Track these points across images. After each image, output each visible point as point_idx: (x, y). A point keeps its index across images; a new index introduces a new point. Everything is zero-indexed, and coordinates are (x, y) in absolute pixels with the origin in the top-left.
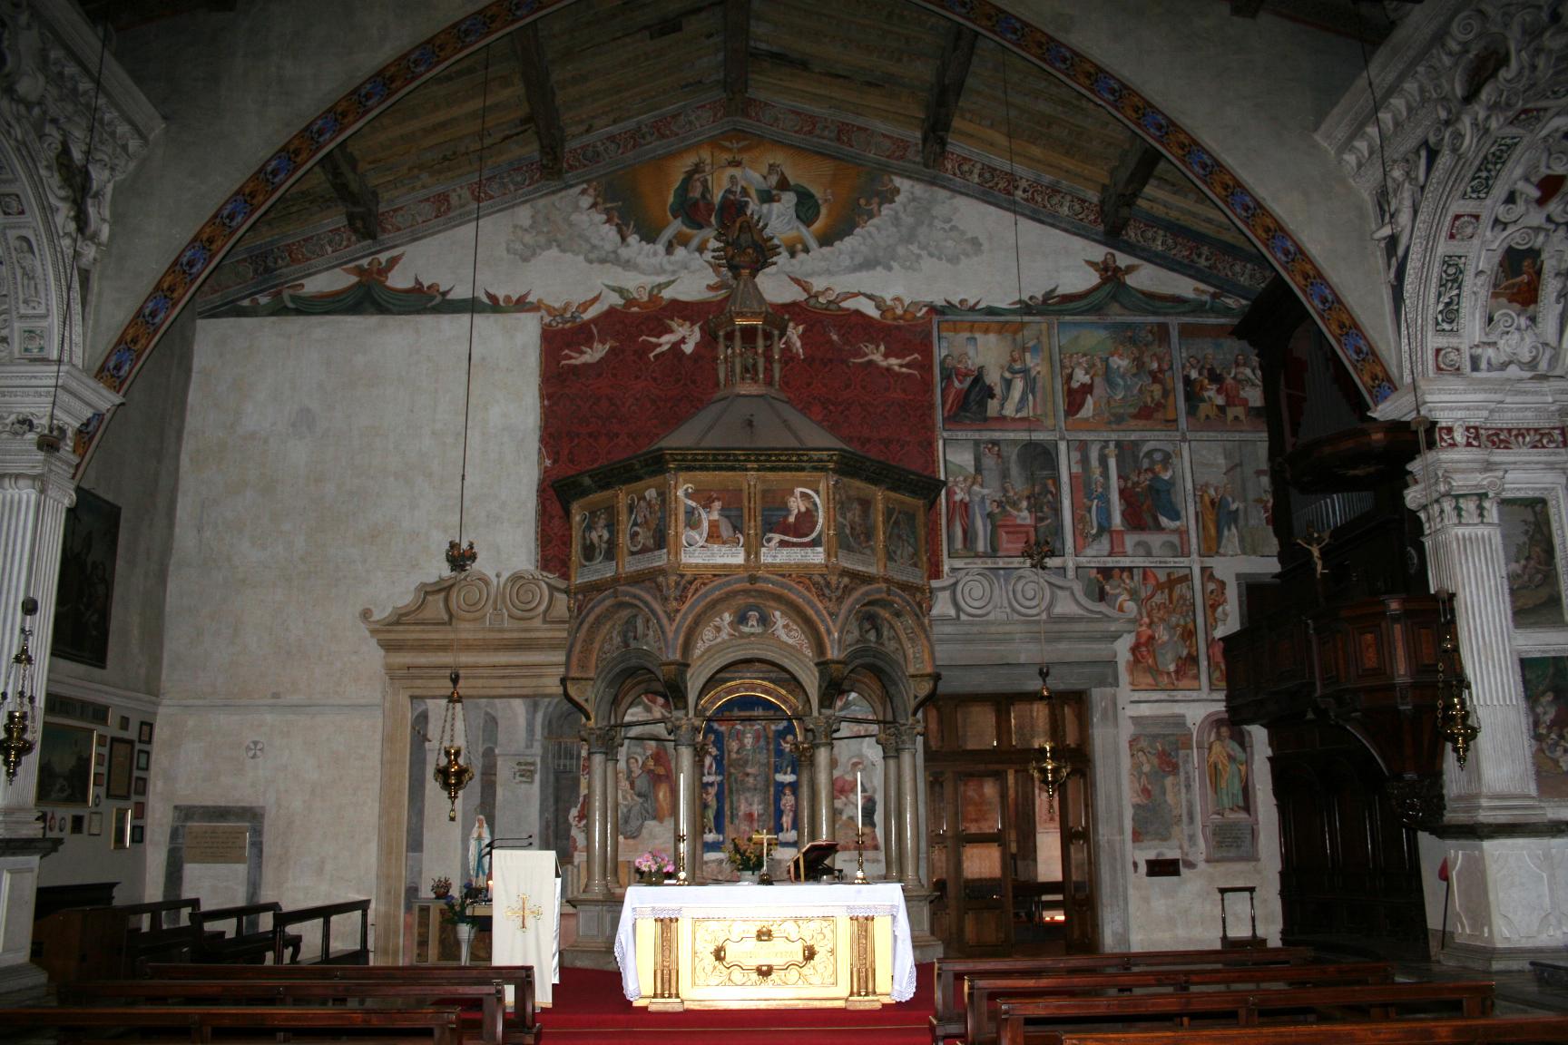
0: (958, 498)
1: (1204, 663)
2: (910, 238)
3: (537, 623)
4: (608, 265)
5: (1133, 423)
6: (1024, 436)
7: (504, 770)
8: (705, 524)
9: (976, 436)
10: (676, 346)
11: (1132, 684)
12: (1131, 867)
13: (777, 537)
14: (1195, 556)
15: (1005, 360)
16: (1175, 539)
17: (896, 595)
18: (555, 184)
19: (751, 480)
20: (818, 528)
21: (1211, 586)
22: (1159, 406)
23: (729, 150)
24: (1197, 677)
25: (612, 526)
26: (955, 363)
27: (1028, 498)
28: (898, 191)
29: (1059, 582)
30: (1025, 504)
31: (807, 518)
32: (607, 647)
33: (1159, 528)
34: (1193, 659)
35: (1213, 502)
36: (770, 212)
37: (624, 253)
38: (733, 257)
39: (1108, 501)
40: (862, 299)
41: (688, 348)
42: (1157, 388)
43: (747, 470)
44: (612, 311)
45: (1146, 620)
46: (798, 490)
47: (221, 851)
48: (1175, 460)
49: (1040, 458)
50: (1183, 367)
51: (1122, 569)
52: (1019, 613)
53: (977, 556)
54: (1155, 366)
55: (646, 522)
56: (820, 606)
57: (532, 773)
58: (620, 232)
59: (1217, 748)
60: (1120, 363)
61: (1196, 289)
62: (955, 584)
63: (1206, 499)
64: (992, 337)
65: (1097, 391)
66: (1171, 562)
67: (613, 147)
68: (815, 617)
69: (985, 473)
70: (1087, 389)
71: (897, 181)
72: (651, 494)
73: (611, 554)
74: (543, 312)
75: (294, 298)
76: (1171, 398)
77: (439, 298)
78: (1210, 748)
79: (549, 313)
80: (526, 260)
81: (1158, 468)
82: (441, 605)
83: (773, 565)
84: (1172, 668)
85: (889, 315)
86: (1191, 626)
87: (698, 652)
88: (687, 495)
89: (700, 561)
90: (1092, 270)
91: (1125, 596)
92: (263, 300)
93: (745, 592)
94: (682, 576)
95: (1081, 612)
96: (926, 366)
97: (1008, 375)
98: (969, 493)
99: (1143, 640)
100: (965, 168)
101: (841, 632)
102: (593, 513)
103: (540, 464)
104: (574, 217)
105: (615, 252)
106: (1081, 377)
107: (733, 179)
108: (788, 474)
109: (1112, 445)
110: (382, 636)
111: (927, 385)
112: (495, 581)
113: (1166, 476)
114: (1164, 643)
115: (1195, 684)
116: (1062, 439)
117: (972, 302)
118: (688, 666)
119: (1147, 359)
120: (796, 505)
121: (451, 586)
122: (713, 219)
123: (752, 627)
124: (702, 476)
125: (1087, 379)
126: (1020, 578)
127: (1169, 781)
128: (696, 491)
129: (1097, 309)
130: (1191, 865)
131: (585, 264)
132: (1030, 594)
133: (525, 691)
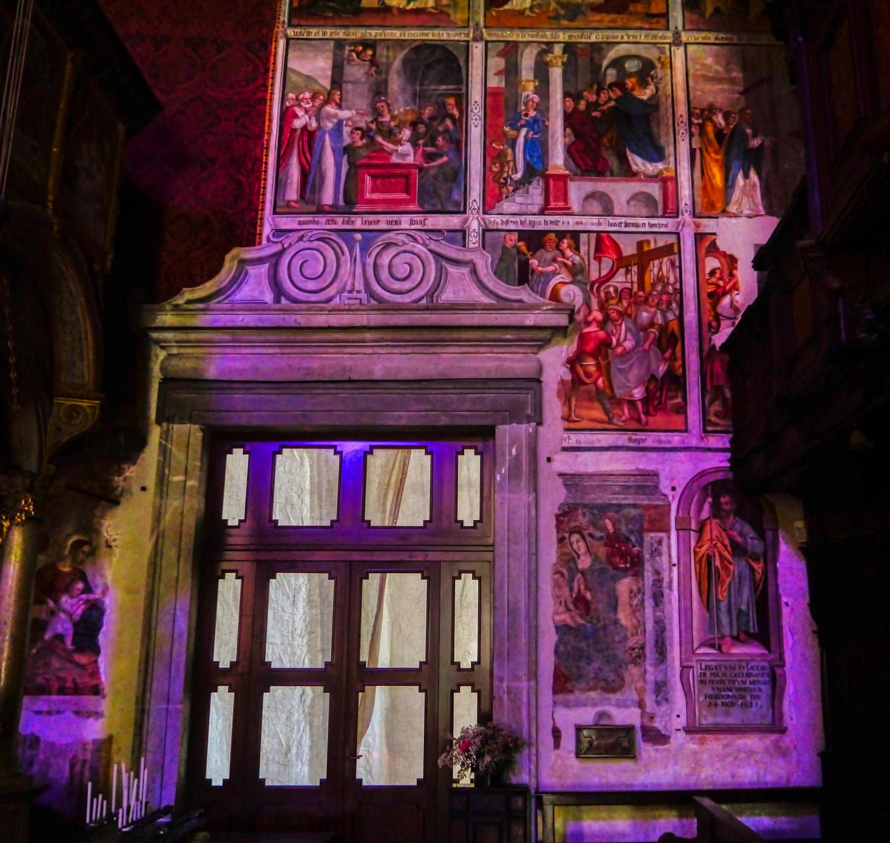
0: (298, 124)
1: (694, 394)
6: (415, 34)
9: (341, 34)
11: (567, 418)
12: (549, 740)
14: (687, 217)
16: (654, 189)
21: (712, 263)
24: (682, 409)
27: (414, 125)
30: (407, 133)
33: (630, 174)
34: (675, 381)
35: (719, 134)
45: (598, 315)
48: (659, 72)
49: (440, 66)
52: (380, 300)
53: (321, 210)
59: (713, 530)
62: (279, 255)
66: (645, 223)
69: (348, 87)
78: (700, 531)
81: (630, 82)
84: (638, 393)
86: (674, 326)
91: (564, 276)
95: (486, 300)
109: (558, 50)
113: (645, 94)
114: (626, 353)
115: (678, 420)
116: (475, 39)
126: (388, 245)
127: (624, 586)
130: (657, 738)
132: (402, 270)
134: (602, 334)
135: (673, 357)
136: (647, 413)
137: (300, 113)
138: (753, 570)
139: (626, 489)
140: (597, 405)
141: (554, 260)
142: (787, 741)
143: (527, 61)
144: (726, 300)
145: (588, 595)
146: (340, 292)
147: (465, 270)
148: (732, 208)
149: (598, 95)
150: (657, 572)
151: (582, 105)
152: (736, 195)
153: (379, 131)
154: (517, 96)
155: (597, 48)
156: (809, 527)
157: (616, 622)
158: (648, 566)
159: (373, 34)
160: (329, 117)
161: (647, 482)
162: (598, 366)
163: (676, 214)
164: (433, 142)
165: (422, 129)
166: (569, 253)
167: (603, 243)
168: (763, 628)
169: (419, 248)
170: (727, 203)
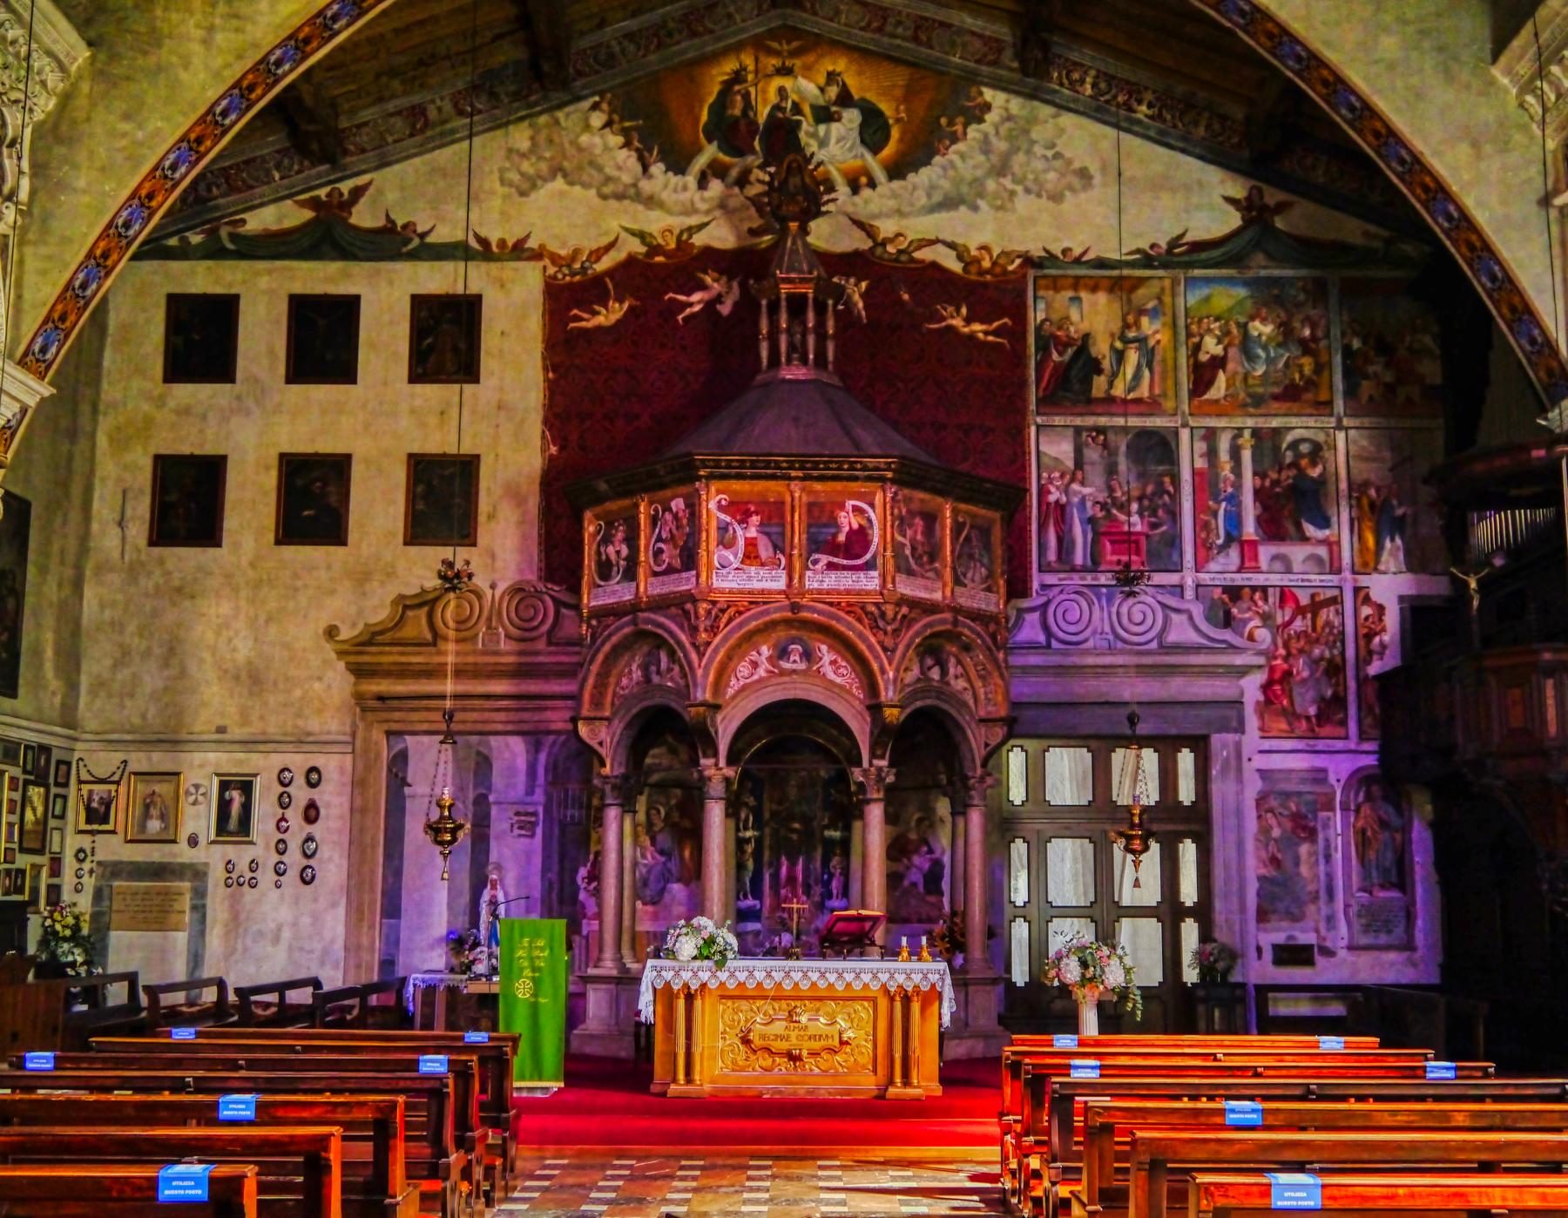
0: (1052, 498)
2: (1001, 170)
3: (541, 645)
4: (626, 202)
5: (1275, 405)
7: (500, 822)
8: (741, 543)
9: (1078, 421)
10: (710, 305)
11: (1261, 729)
12: (1253, 953)
13: (825, 559)
14: (1347, 574)
15: (1116, 326)
16: (1322, 552)
17: (965, 625)
18: (556, 96)
19: (797, 493)
20: (873, 548)
21: (1366, 611)
22: (1311, 384)
23: (777, 53)
24: (1343, 723)
25: (632, 540)
26: (1054, 329)
27: (1140, 499)
28: (987, 107)
29: (1172, 602)
30: (1135, 506)
31: (860, 538)
32: (625, 681)
33: (1304, 539)
34: (1339, 701)
36: (828, 133)
37: (646, 186)
38: (779, 206)
39: (1239, 504)
40: (940, 248)
41: (725, 309)
42: (1307, 363)
43: (790, 478)
44: (631, 260)
45: (1282, 651)
46: (850, 503)
47: (156, 917)
48: (1327, 454)
49: (1156, 449)
50: (1343, 334)
51: (1254, 589)
52: (1125, 641)
53: (1074, 569)
54: (1307, 332)
55: (672, 536)
56: (873, 640)
57: (534, 824)
58: (641, 158)
59: (1366, 810)
60: (1262, 329)
61: (1366, 234)
62: (1046, 605)
63: (1365, 502)
64: (1102, 298)
65: (1230, 366)
66: (1316, 579)
67: (632, 48)
68: (867, 653)
69: (1087, 468)
70: (1218, 363)
71: (988, 94)
72: (678, 504)
73: (630, 574)
74: (547, 262)
75: (234, 237)
76: (1326, 374)
77: (416, 242)
78: (1357, 811)
79: (554, 262)
80: (523, 194)
81: (1304, 462)
82: (424, 621)
83: (820, 592)
84: (1312, 711)
85: (973, 269)
86: (1338, 660)
87: (730, 692)
88: (720, 508)
89: (734, 585)
90: (1231, 209)
91: (1257, 622)
92: (196, 239)
93: (787, 623)
94: (714, 603)
96: (1017, 332)
97: (1118, 345)
98: (1066, 491)
99: (1277, 675)
100: (1076, 76)
101: (897, 670)
102: (610, 525)
103: (543, 451)
104: (584, 139)
105: (635, 185)
106: (1212, 347)
107: (782, 91)
108: (838, 485)
109: (1247, 434)
110: (352, 659)
111: (1017, 358)
112: (489, 592)
113: (1315, 472)
114: (1304, 681)
115: (1340, 731)
116: (1185, 425)
117: (1077, 252)
118: (717, 708)
119: (1297, 325)
120: (847, 521)
121: (437, 599)
122: (756, 143)
123: (794, 662)
124: (736, 485)
125: (1218, 350)
127: (1304, 849)
128: (731, 503)
129: (1235, 260)
130: (1328, 953)
131: (597, 201)
132: (1138, 617)
133: (525, 727)
134: (1286, 666)
135: (1337, 684)
136: (1319, 725)
137: (1053, 489)
138: (1394, 839)
139: (1304, 781)
140: (1282, 719)
141: (1249, 609)
142: (1417, 955)
143: (1224, 445)
144: (1377, 640)
145: (1279, 856)
146: (1094, 633)
147: (1184, 617)
148: (1382, 567)
149: (1279, 472)
150: (1327, 841)
151: (1267, 483)
152: (1385, 556)
153: (1114, 504)
154: (1217, 475)
155: (1277, 433)
156: (1435, 809)
157: (1299, 874)
158: (1321, 836)
159: (1103, 421)
160: (1076, 493)
161: (1319, 776)
162: (1283, 690)
163: (1339, 571)
164: (1154, 513)
165: (1146, 502)
166: (1260, 603)
167: (1286, 595)
168: (1400, 878)
169: (1149, 600)
170: (1377, 562)
